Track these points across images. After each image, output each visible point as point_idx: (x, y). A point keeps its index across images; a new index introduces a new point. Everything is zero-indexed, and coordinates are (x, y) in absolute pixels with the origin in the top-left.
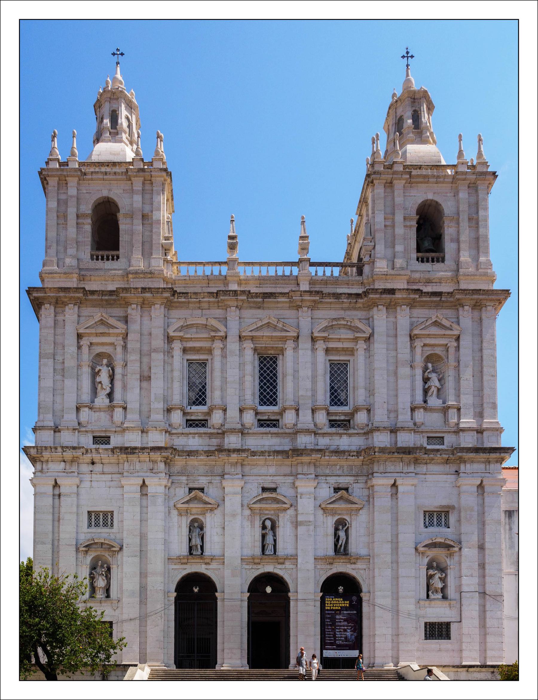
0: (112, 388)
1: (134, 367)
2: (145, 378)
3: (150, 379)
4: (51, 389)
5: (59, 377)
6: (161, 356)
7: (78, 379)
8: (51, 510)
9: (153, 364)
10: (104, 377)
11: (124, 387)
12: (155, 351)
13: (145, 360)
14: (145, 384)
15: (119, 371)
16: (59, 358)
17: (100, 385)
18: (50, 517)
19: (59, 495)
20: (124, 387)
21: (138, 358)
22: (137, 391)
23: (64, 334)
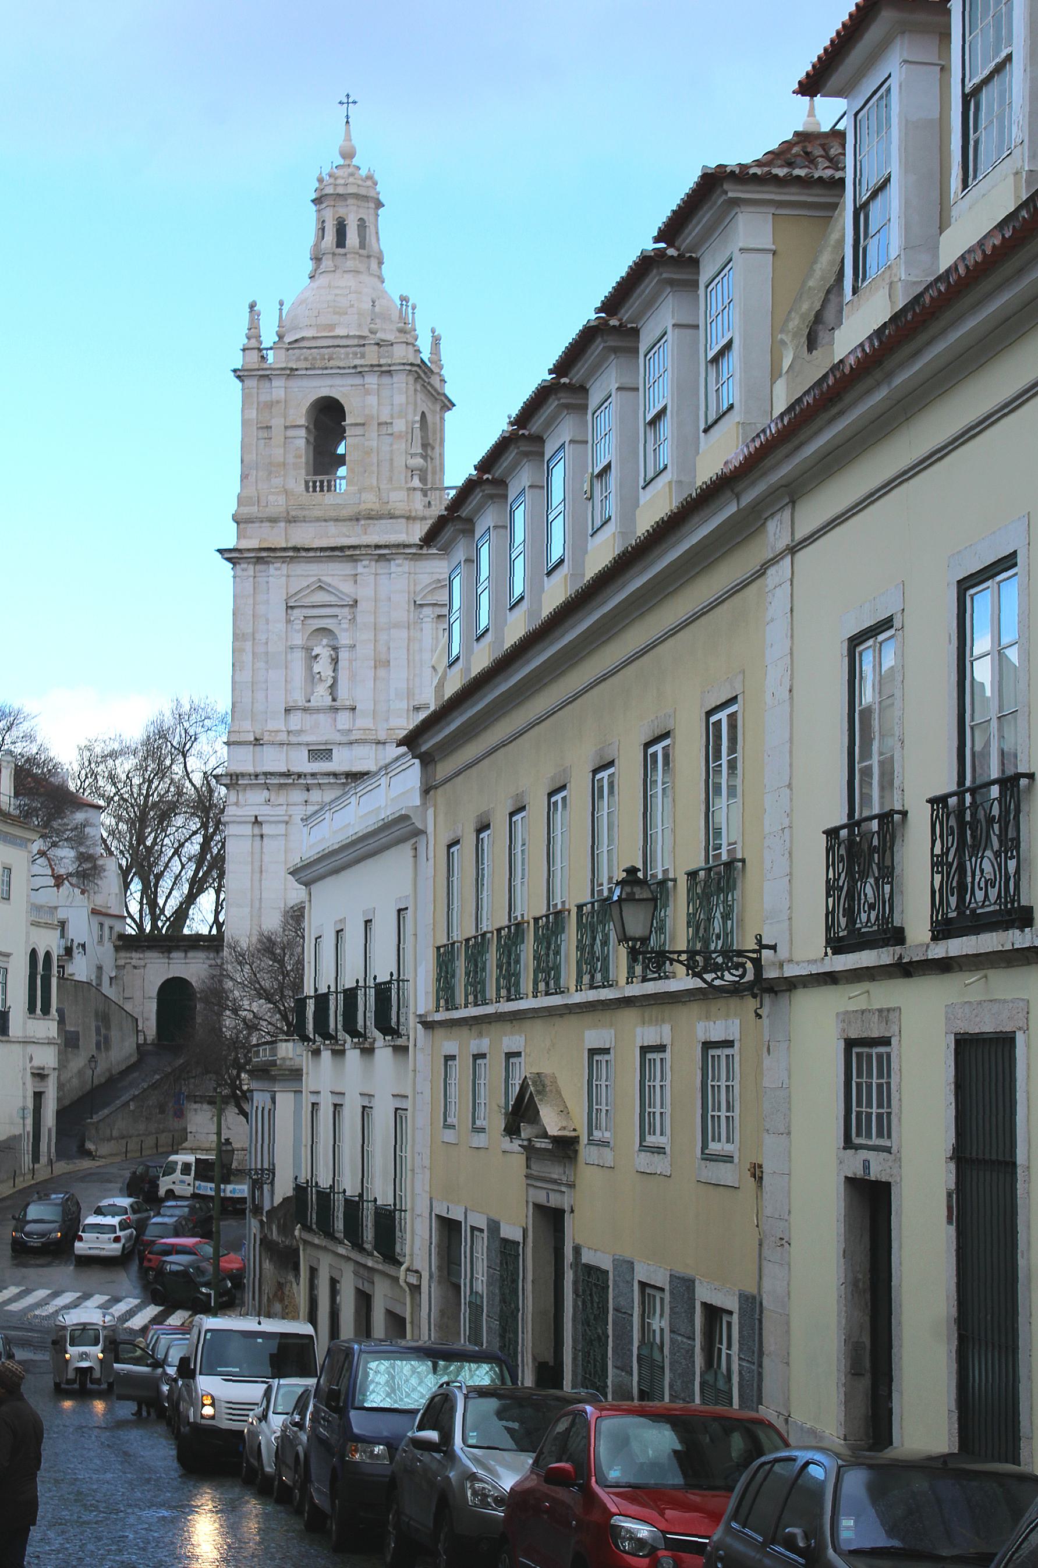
0: (335, 680)
1: (365, 650)
2: (381, 663)
3: (389, 665)
4: (250, 685)
5: (260, 665)
6: (404, 634)
7: (286, 668)
8: (250, 859)
9: (392, 645)
10: (323, 667)
11: (353, 677)
12: (397, 626)
13: (383, 637)
14: (382, 672)
15: (343, 655)
16: (261, 637)
17: (318, 676)
18: (249, 868)
19: (262, 836)
20: (353, 677)
21: (372, 638)
22: (370, 684)
23: (267, 602)
